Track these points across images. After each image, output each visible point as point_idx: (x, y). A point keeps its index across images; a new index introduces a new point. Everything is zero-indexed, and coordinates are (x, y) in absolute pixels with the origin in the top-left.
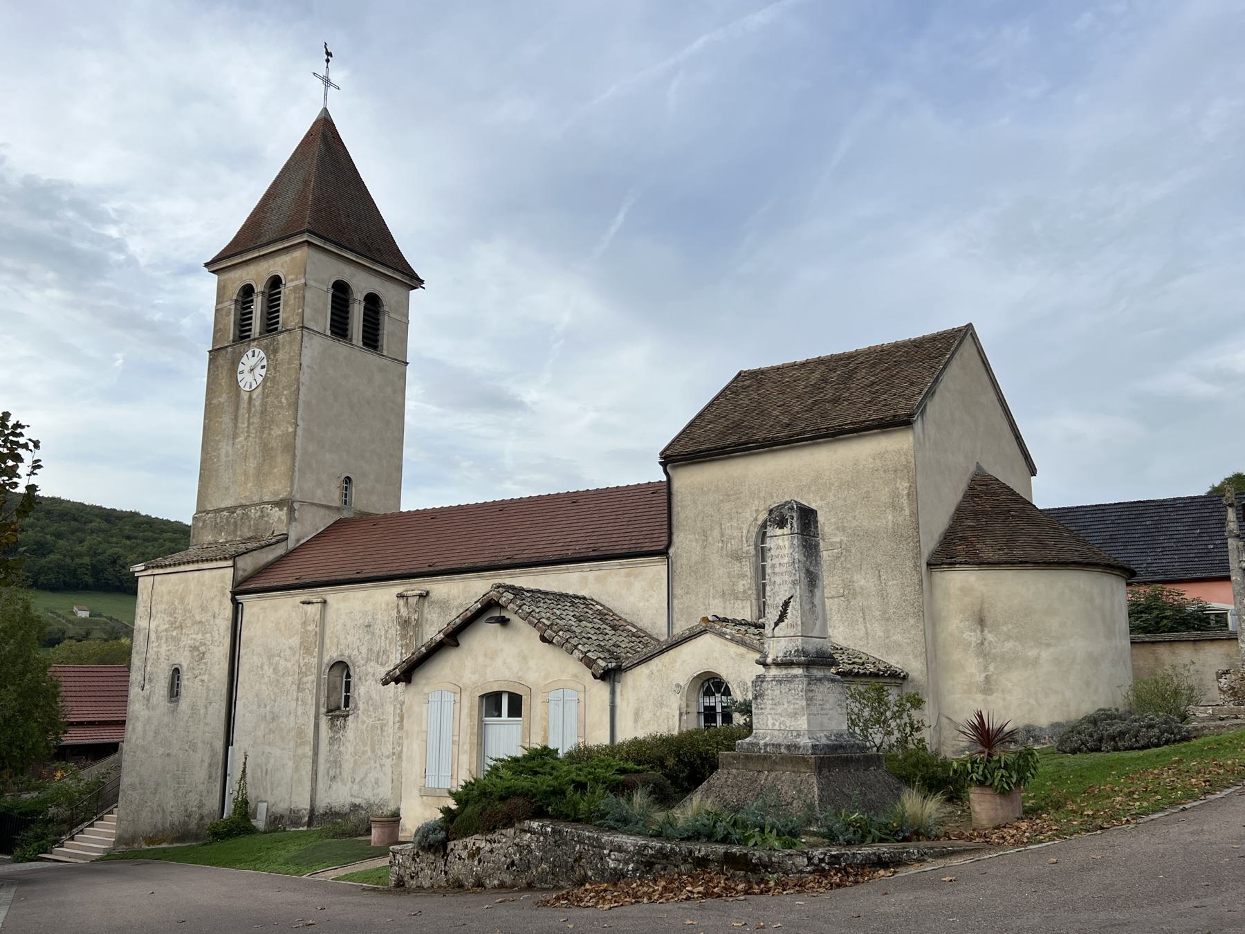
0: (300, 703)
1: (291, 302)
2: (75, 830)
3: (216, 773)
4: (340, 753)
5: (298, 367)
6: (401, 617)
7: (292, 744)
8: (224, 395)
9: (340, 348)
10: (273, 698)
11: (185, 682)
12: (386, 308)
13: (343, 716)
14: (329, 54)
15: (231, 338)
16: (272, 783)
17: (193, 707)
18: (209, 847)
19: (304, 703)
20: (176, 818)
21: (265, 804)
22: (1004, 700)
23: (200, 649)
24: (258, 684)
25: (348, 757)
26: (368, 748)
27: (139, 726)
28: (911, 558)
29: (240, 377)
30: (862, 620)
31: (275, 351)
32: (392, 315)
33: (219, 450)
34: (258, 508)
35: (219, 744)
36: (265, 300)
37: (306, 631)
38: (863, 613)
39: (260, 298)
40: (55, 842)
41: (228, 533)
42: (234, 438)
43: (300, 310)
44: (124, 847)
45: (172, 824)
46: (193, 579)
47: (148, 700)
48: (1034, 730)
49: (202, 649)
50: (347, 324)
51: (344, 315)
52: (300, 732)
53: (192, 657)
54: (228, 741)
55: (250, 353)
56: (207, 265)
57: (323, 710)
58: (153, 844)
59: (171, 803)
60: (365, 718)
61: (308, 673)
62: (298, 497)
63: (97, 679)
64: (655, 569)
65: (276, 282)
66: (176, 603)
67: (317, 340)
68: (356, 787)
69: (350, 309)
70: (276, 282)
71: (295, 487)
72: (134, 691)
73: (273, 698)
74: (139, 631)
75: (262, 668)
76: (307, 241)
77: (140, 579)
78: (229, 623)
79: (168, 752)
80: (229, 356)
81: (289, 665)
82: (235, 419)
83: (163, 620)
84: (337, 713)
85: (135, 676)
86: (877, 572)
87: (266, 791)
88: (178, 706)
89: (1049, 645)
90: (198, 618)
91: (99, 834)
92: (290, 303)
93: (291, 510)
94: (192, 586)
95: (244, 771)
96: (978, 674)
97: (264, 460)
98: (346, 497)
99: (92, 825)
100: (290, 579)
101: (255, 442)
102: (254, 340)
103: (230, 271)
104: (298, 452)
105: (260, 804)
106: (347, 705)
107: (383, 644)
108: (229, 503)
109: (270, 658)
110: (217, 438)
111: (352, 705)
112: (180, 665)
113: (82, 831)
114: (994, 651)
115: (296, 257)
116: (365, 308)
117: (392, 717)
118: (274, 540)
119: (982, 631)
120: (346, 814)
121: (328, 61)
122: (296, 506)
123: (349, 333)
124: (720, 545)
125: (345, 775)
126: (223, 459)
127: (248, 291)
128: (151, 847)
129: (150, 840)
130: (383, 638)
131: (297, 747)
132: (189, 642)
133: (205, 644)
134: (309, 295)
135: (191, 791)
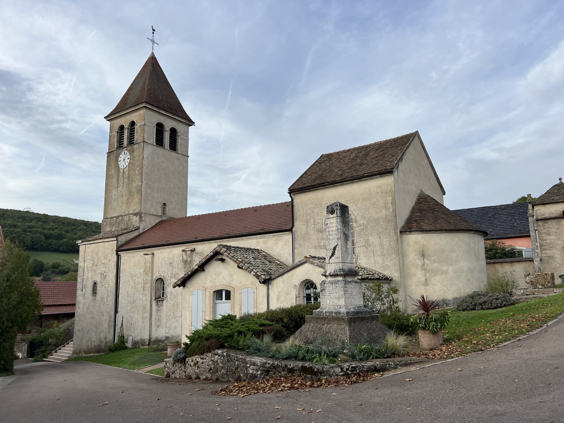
0: (144, 295)
1: (139, 131)
3: (112, 325)
4: (161, 316)
5: (142, 158)
6: (184, 259)
7: (141, 312)
8: (113, 171)
9: (160, 150)
10: (133, 293)
11: (98, 288)
12: (179, 134)
14: (153, 30)
15: (116, 147)
16: (134, 329)
17: (102, 298)
18: (107, 355)
19: (146, 296)
20: (96, 343)
21: (131, 337)
22: (433, 288)
25: (164, 317)
27: (81, 306)
28: (393, 229)
29: (119, 163)
30: (373, 256)
31: (133, 152)
32: (181, 137)
33: (112, 193)
34: (127, 216)
35: (113, 313)
36: (129, 131)
37: (146, 266)
38: (373, 253)
39: (127, 130)
40: (49, 353)
41: (116, 227)
42: (118, 187)
43: (143, 135)
44: (76, 355)
47: (84, 296)
48: (446, 301)
49: (105, 274)
50: (163, 141)
51: (161, 137)
52: (144, 307)
53: (101, 277)
54: (116, 312)
55: (123, 153)
56: (105, 118)
57: (154, 298)
58: (87, 354)
59: (94, 337)
61: (147, 283)
62: (143, 211)
63: (72, 287)
64: (287, 237)
65: (133, 124)
66: (95, 256)
67: (150, 147)
68: (167, 329)
69: (164, 134)
70: (133, 124)
71: (142, 207)
72: (79, 292)
73: (133, 293)
74: (80, 267)
75: (129, 282)
76: (145, 106)
77: (80, 246)
78: (115, 264)
81: (140, 280)
82: (118, 180)
83: (90, 263)
84: (159, 299)
85: (79, 286)
86: (379, 236)
87: (131, 332)
88: (96, 297)
89: (452, 265)
90: (103, 262)
91: (67, 350)
92: (139, 132)
93: (141, 217)
94: (101, 248)
95: (122, 324)
96: (422, 278)
97: (130, 197)
98: (164, 211)
99: (64, 346)
100: (139, 245)
101: (126, 189)
102: (125, 148)
104: (143, 193)
105: (129, 337)
106: (163, 296)
107: (177, 271)
108: (116, 214)
109: (132, 277)
111: (165, 296)
113: (60, 349)
114: (429, 268)
116: (170, 134)
117: (181, 301)
118: (133, 229)
119: (424, 260)
121: (153, 33)
122: (143, 215)
123: (164, 144)
124: (314, 226)
125: (163, 324)
126: (113, 197)
127: (122, 128)
128: (87, 355)
129: (86, 352)
132: (100, 271)
133: (106, 272)
134: (146, 128)
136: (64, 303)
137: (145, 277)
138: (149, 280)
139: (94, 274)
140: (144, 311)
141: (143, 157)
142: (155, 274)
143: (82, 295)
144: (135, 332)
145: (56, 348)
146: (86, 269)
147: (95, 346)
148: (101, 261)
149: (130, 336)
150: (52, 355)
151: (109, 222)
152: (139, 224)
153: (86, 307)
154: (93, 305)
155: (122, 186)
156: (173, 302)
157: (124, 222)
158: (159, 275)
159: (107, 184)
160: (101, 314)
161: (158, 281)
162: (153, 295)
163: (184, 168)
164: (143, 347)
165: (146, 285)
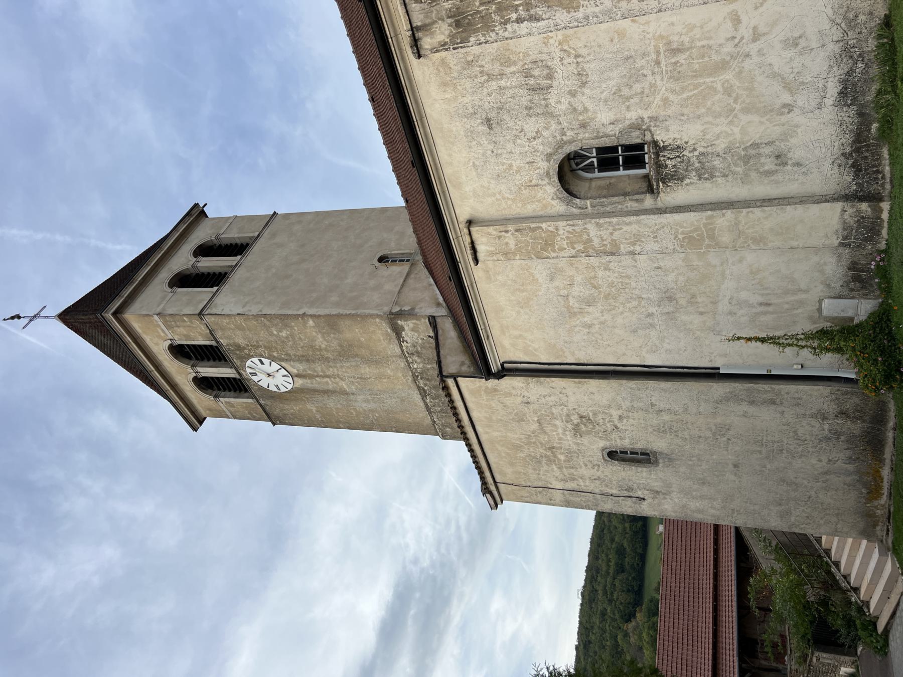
0: (637, 248)
2: (844, 585)
3: (766, 392)
4: (728, 150)
6: (452, 37)
7: (713, 258)
8: (309, 407)
10: (635, 303)
11: (626, 443)
13: (657, 155)
15: (250, 401)
16: (787, 292)
17: (661, 431)
19: (637, 239)
20: (839, 454)
21: (826, 302)
23: (575, 422)
24: (617, 331)
25: (736, 130)
26: (718, 82)
27: (694, 505)
29: (283, 390)
31: (239, 347)
32: (222, 231)
33: (365, 410)
34: (410, 360)
35: (718, 389)
37: (518, 250)
40: (860, 610)
42: (344, 393)
44: (878, 528)
45: (850, 460)
46: (487, 433)
47: (657, 492)
49: (575, 419)
52: (691, 241)
53: (589, 433)
54: (712, 375)
55: (255, 378)
57: (649, 201)
58: (881, 488)
59: (814, 461)
60: (658, 100)
61: (585, 237)
63: (675, 535)
65: (180, 351)
66: (522, 455)
68: (801, 100)
70: (180, 351)
71: (375, 312)
73: (635, 303)
75: (590, 326)
78: (532, 381)
79: (731, 466)
80: (269, 403)
81: (578, 279)
83: (547, 471)
87: (801, 303)
88: (661, 453)
90: (535, 426)
93: (401, 314)
94: (496, 434)
97: (357, 355)
99: (837, 564)
101: (341, 367)
103: (192, 405)
105: (825, 313)
109: (573, 314)
110: (354, 413)
112: (603, 450)
115: (139, 326)
120: (861, 115)
122: (396, 309)
125: (775, 132)
126: (372, 406)
127: (204, 384)
128: (885, 491)
129: (874, 492)
130: (502, 83)
131: (718, 245)
132: (569, 438)
133: (568, 415)
134: (170, 311)
135: (796, 433)
136: (712, 553)
137: (562, 249)
138: (570, 229)
139: (580, 457)
140: (707, 242)
141: (238, 314)
142: (545, 206)
143: (656, 501)
144: (803, 286)
145: (840, 588)
146: (571, 485)
147: (850, 460)
148: (533, 432)
149: (819, 310)
150: (867, 604)
151: (442, 417)
152: (423, 320)
153: (696, 487)
154: (690, 463)
155: (338, 379)
156: (658, 78)
157: (428, 370)
158: (546, 181)
159: (347, 425)
160: (723, 435)
161: (572, 188)
162: (634, 205)
163: (300, 222)
164: (884, 232)
165: (591, 240)
